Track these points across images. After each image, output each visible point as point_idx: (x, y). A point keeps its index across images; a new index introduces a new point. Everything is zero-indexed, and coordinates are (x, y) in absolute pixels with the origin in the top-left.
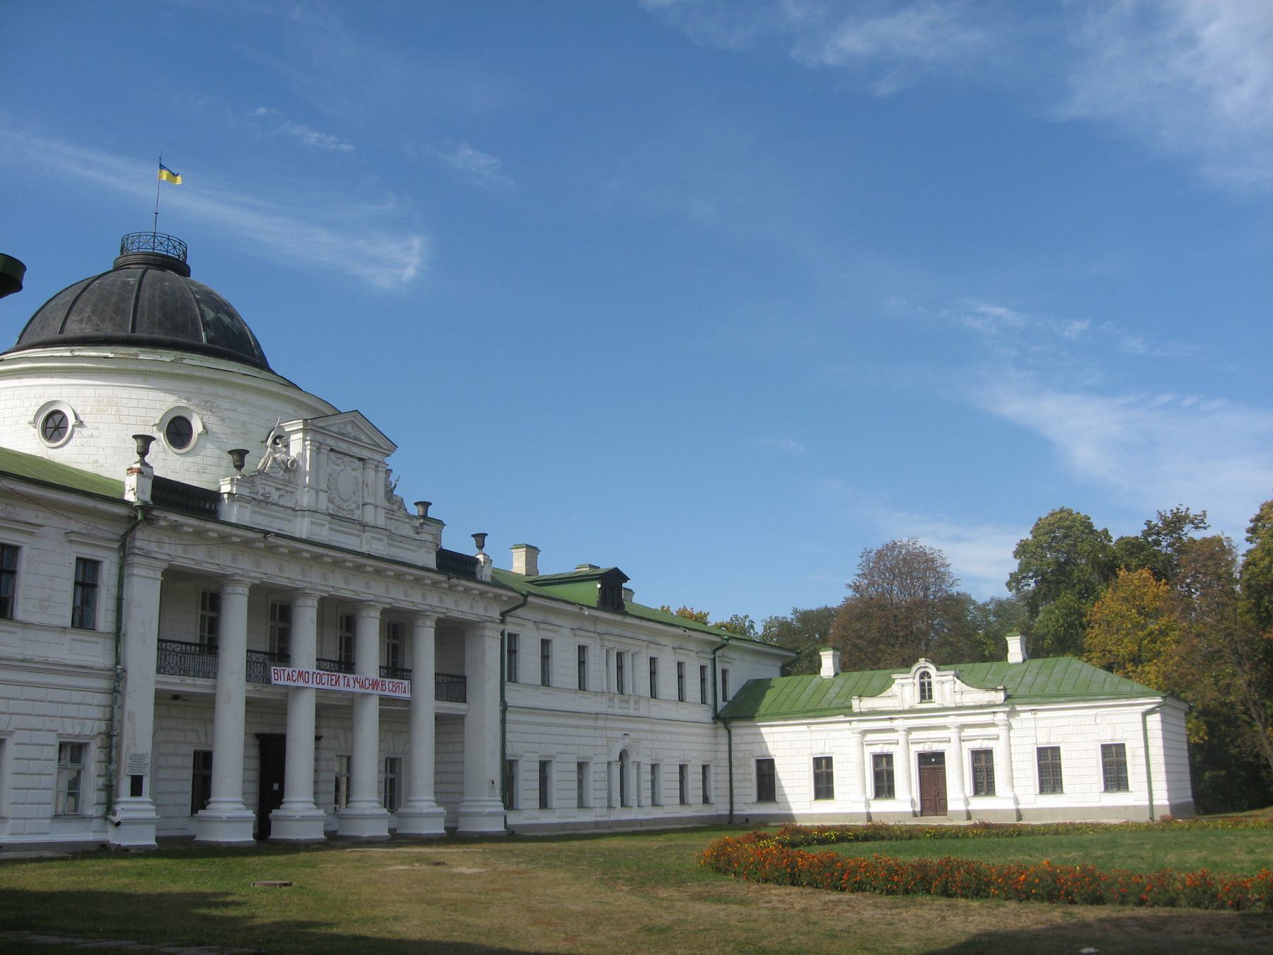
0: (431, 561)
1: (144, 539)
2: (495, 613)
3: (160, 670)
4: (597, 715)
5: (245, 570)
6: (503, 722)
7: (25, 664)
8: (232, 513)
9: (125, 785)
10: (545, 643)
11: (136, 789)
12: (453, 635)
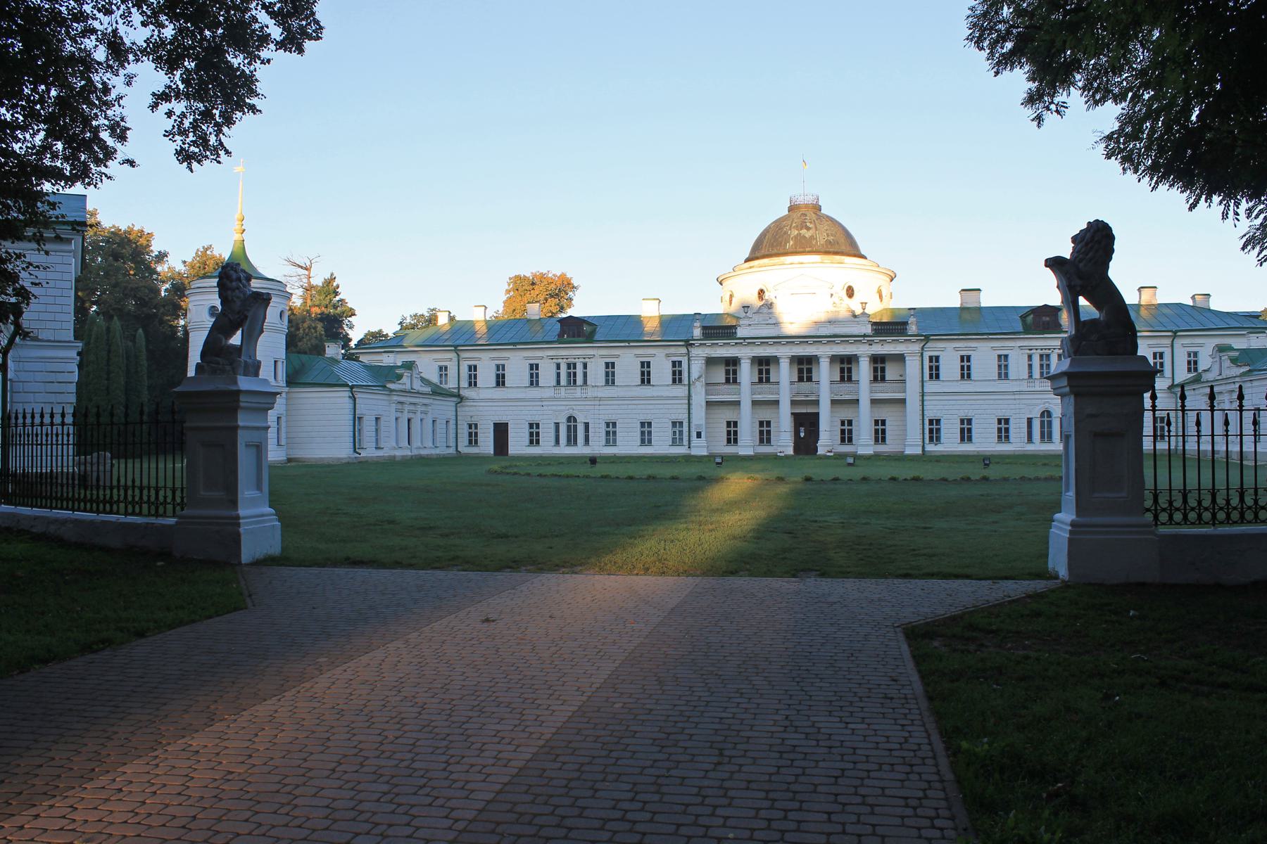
0: (868, 330)
1: (695, 351)
2: (916, 347)
3: (707, 393)
4: (1014, 393)
5: (746, 354)
6: (923, 401)
7: (653, 398)
8: (741, 332)
9: (694, 434)
10: (966, 359)
11: (699, 435)
12: (878, 361)
